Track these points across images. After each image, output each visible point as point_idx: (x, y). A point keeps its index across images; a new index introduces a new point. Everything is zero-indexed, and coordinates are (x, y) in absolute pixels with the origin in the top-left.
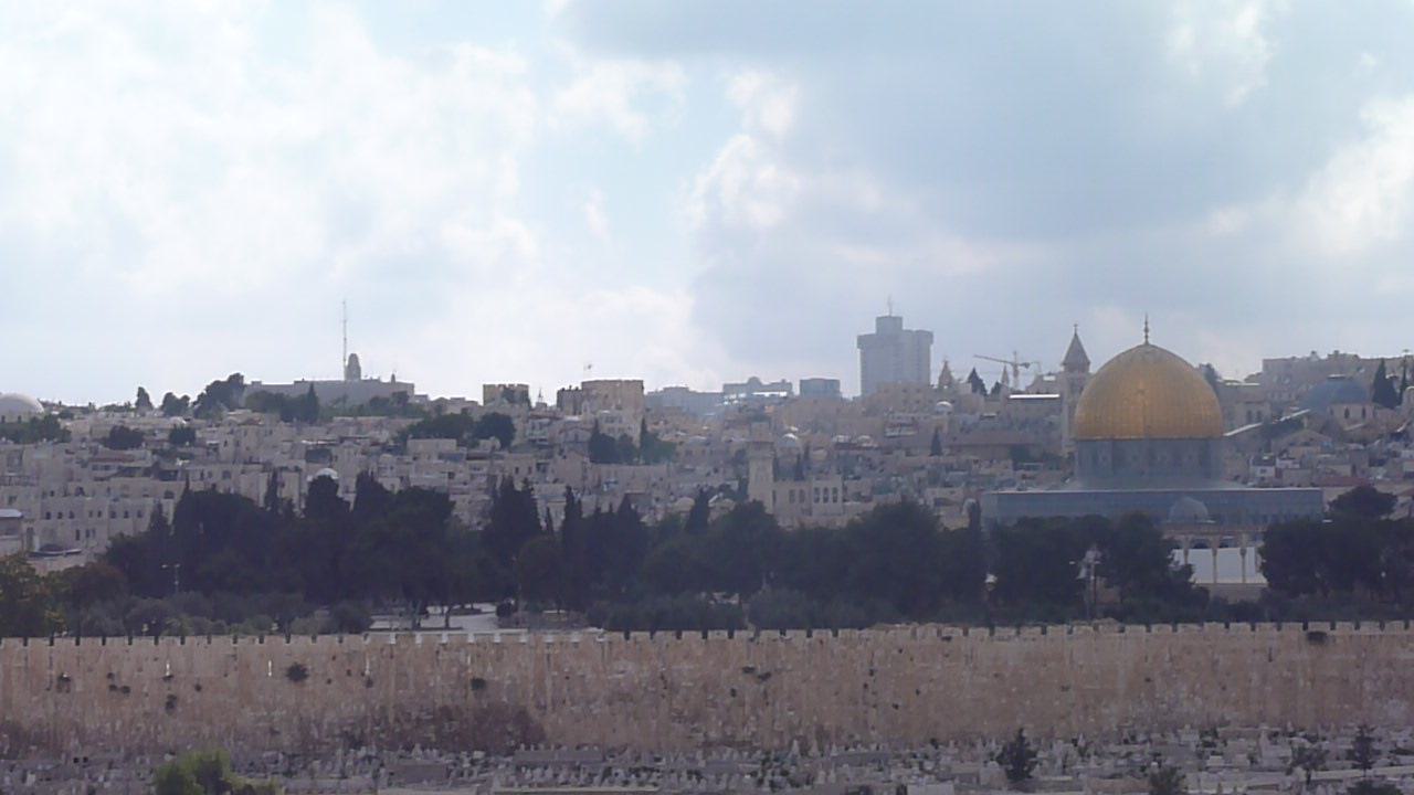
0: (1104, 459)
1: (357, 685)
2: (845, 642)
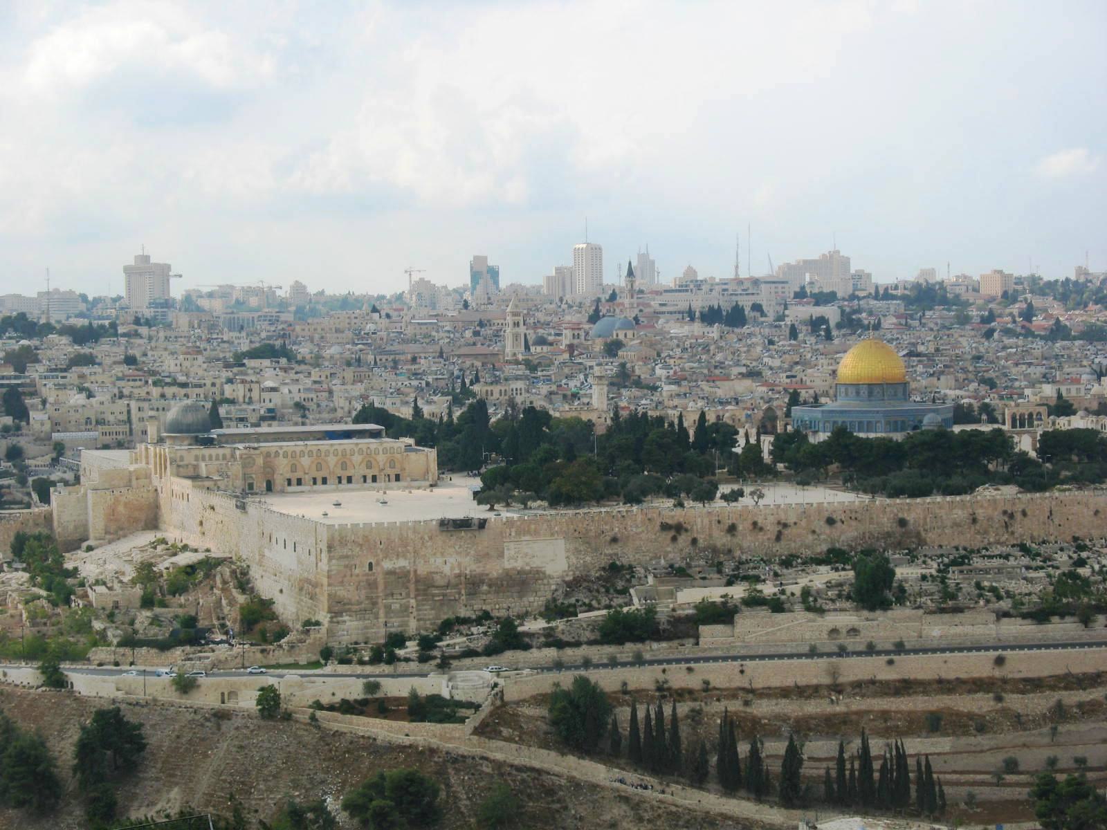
1: (854, 523)
2: (1041, 498)
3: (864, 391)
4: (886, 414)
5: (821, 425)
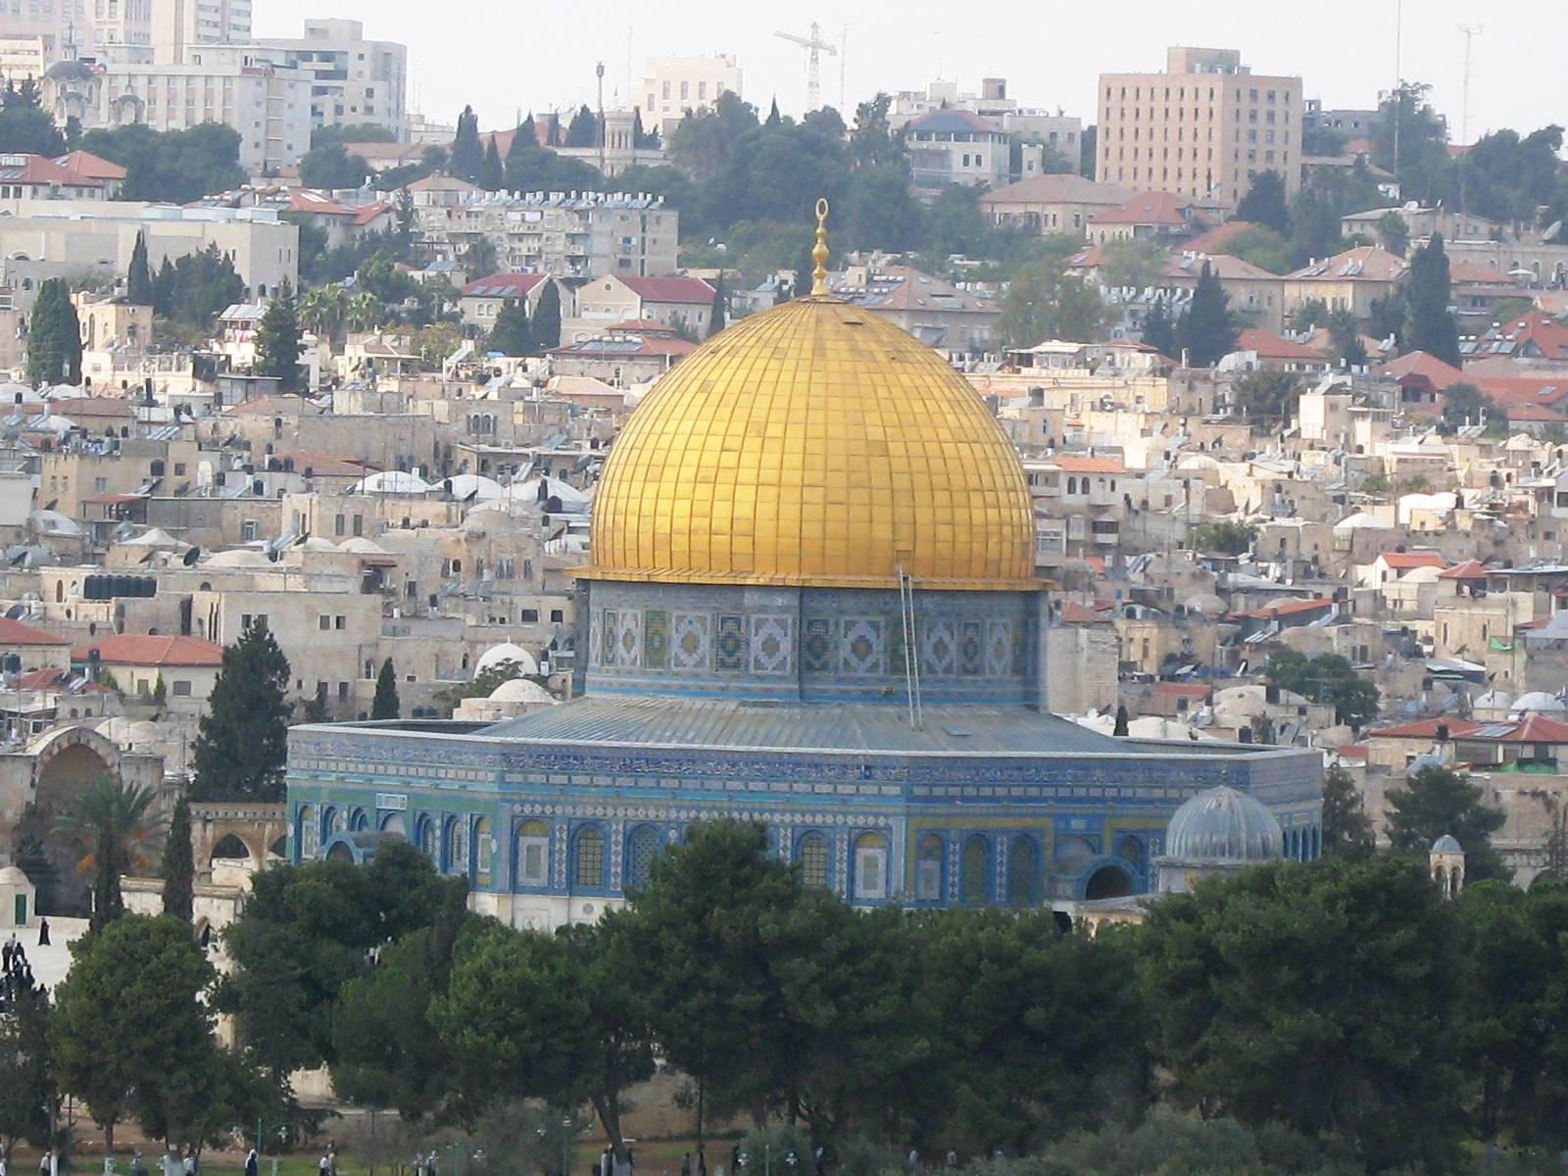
0: (771, 647)
3: (772, 637)
4: (924, 779)
5: (492, 845)
